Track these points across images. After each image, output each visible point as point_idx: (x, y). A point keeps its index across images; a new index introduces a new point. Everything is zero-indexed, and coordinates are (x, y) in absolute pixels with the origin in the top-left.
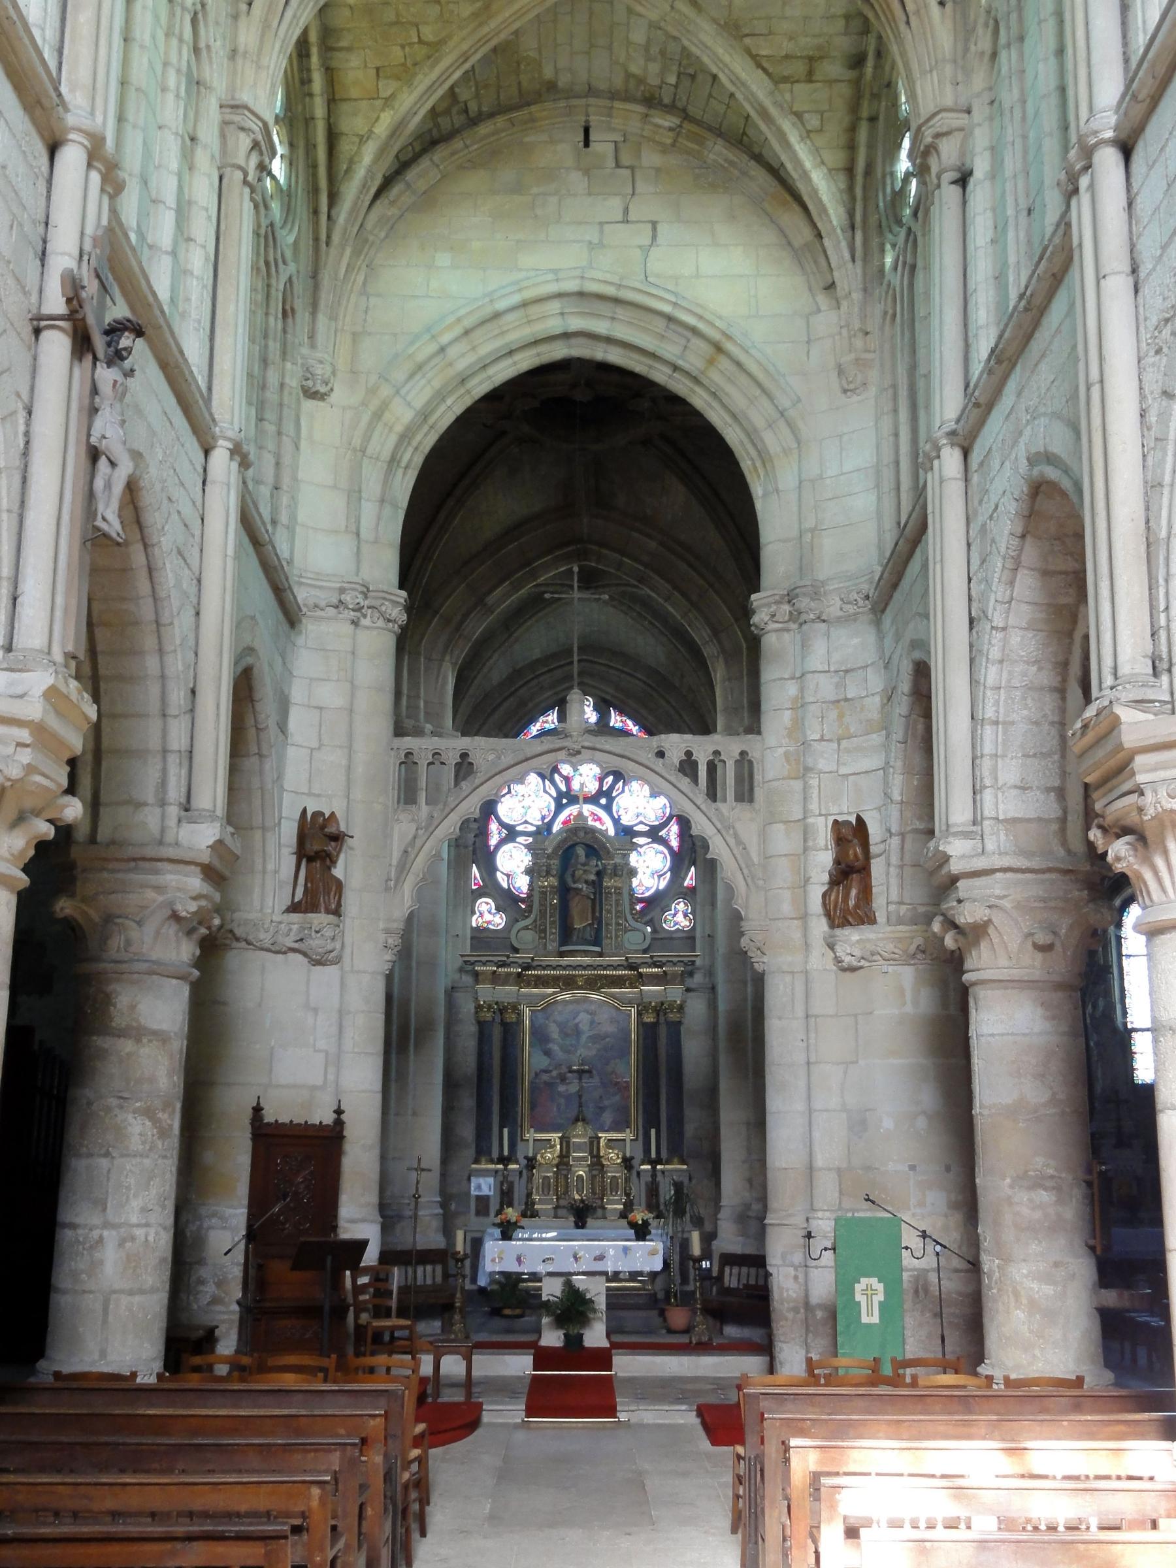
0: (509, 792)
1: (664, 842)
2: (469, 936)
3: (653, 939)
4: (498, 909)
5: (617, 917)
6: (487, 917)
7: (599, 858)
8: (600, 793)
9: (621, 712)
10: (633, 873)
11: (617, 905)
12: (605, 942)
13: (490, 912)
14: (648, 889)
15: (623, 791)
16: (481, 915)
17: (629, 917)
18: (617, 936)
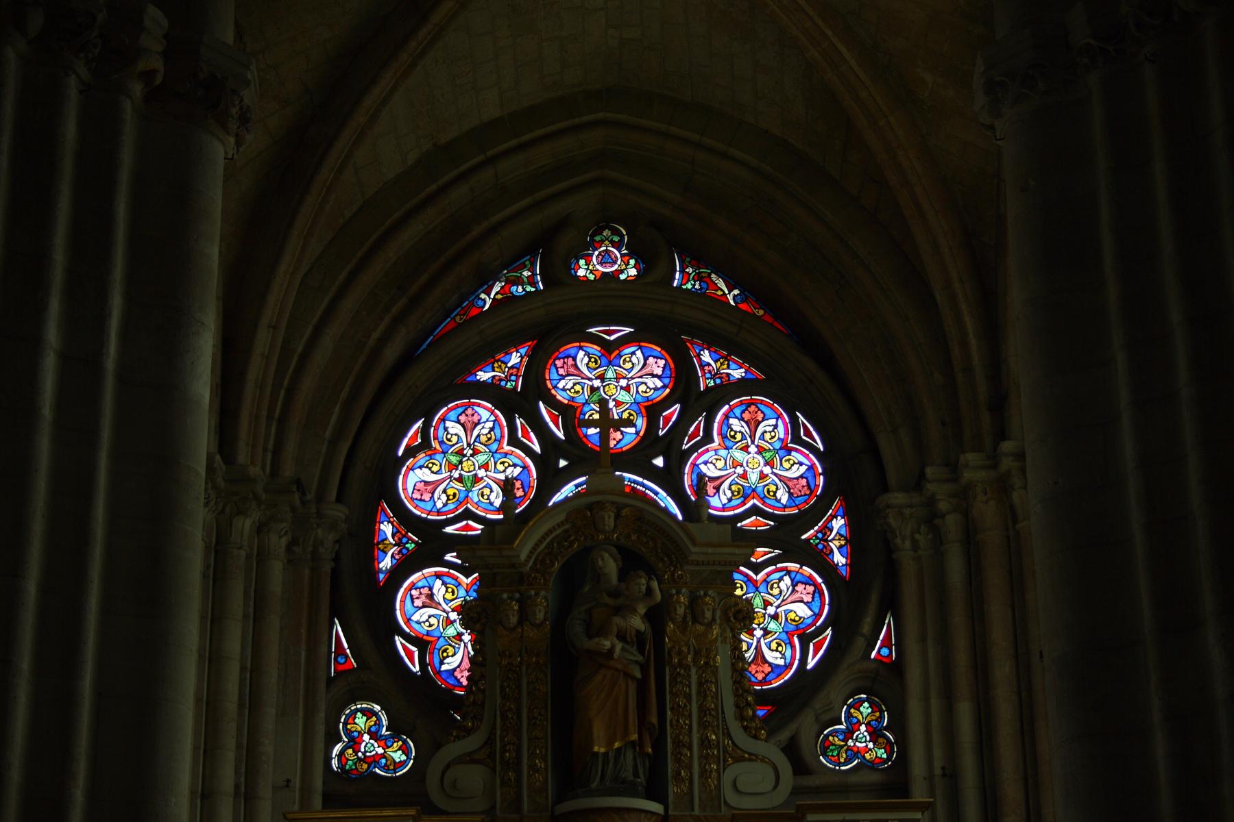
0: (425, 445)
1: (817, 558)
2: (318, 783)
3: (796, 791)
4: (396, 730)
5: (703, 725)
6: (369, 746)
7: (651, 572)
8: (649, 444)
9: (697, 257)
10: (743, 616)
11: (702, 694)
12: (673, 789)
13: (374, 735)
14: (778, 670)
15: (708, 438)
16: (354, 742)
17: (735, 728)
18: (704, 773)
